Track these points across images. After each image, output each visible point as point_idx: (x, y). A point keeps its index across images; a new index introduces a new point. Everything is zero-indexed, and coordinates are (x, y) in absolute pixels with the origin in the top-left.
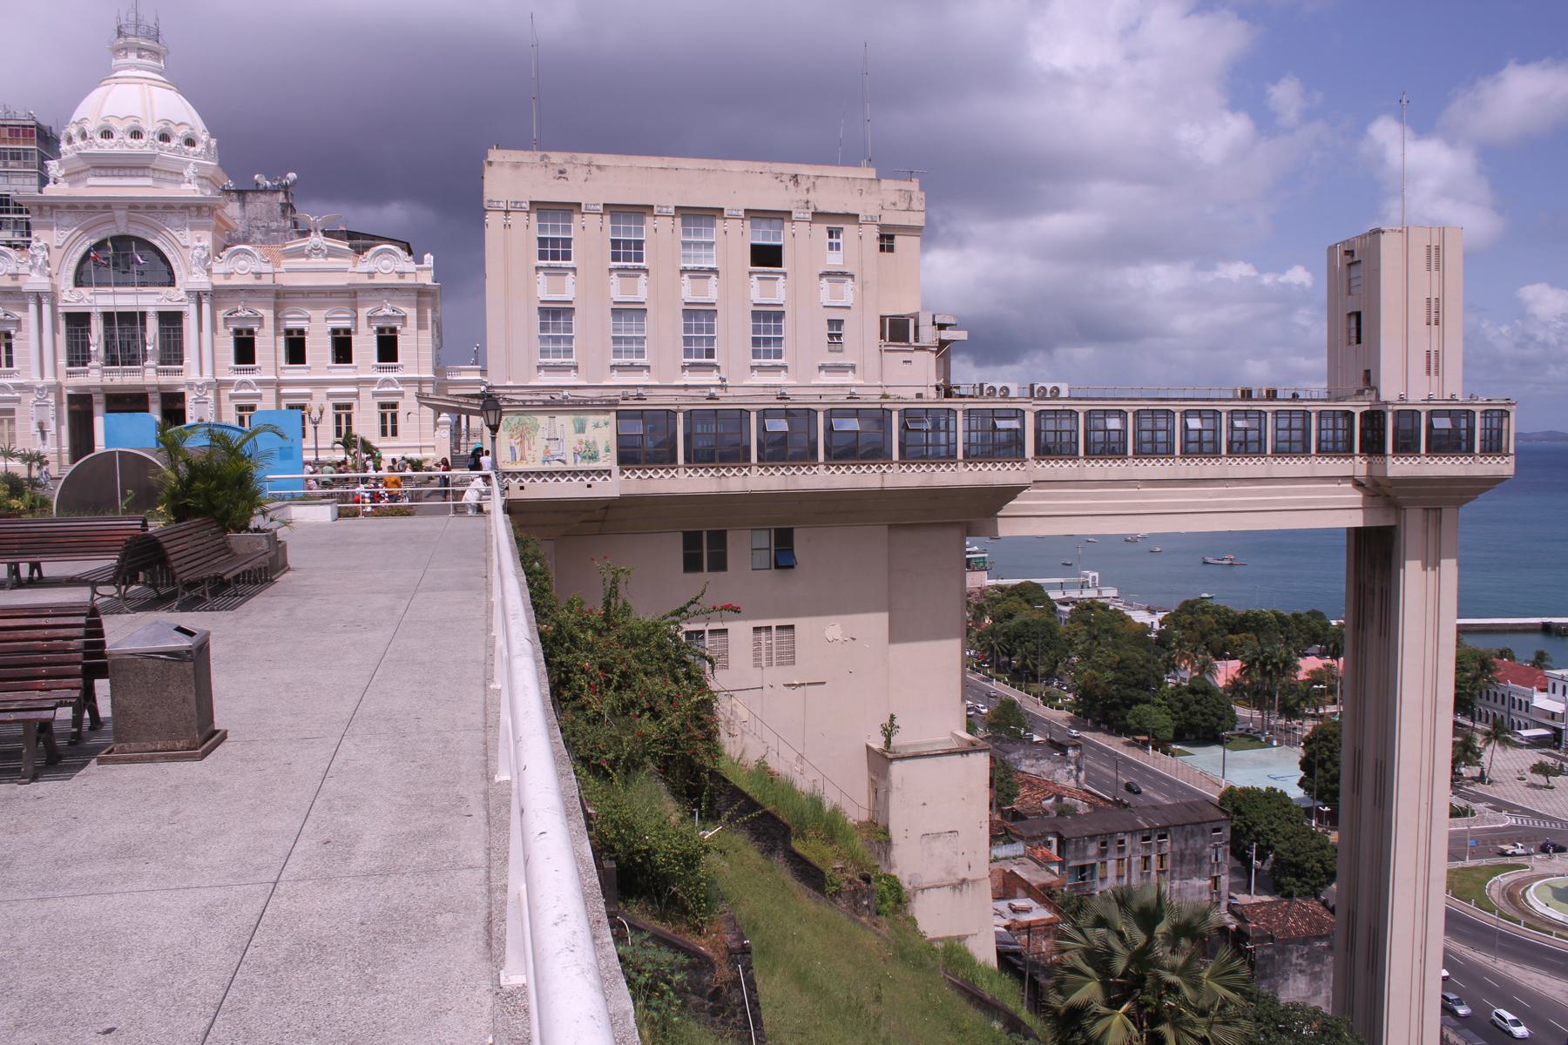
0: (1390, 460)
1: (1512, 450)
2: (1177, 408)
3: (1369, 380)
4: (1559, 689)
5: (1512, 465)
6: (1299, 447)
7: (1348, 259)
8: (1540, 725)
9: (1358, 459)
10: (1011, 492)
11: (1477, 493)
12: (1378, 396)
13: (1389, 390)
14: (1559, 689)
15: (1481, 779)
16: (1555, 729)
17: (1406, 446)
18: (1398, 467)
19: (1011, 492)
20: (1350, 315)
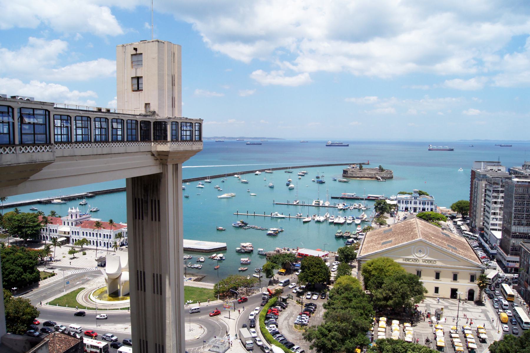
4: (66, 224)
7: (134, 52)
8: (62, 237)
9: (153, 143)
14: (66, 224)
16: (66, 237)
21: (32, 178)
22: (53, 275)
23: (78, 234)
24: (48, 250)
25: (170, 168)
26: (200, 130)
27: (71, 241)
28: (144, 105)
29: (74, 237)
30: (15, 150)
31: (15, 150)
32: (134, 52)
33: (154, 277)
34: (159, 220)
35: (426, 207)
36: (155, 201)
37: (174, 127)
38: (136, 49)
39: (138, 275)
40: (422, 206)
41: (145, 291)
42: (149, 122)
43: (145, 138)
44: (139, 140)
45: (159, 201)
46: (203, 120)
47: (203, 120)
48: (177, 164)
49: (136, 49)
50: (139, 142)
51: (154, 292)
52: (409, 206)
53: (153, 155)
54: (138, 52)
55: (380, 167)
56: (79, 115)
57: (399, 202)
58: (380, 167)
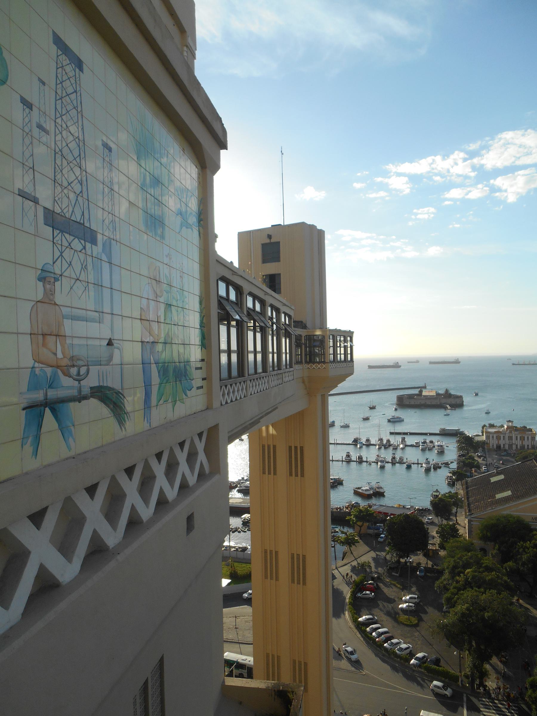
26: (351, 347)
32: (268, 241)
33: (293, 558)
34: (302, 475)
35: (526, 443)
36: (296, 448)
38: (270, 237)
39: (266, 557)
40: (519, 443)
41: (277, 579)
42: (301, 336)
46: (353, 333)
47: (353, 333)
49: (270, 237)
51: (293, 582)
52: (502, 442)
53: (303, 382)
54: (272, 241)
55: (447, 391)
57: (487, 437)
58: (447, 391)
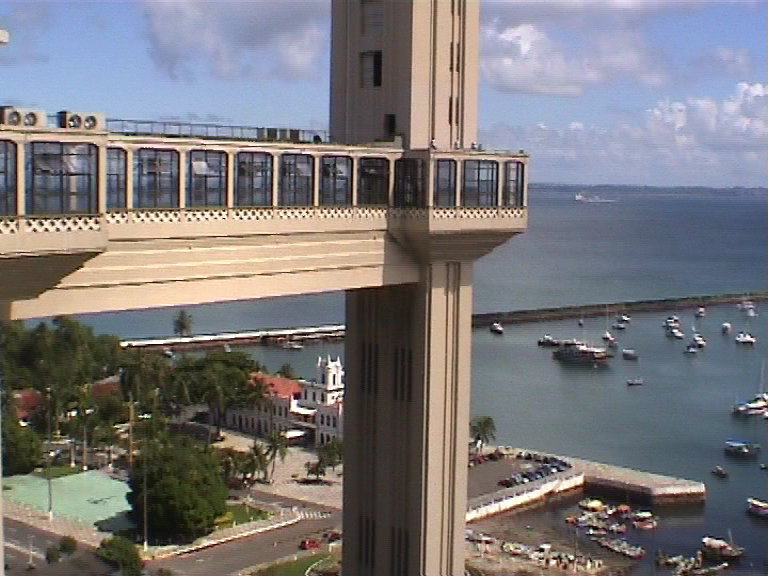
0: (432, 213)
1: (525, 204)
2: (183, 147)
3: (393, 127)
5: (525, 218)
6: (341, 197)
10: (75, 260)
11: (490, 247)
12: (406, 144)
13: (418, 140)
14: (310, 396)
15: (264, 481)
16: (307, 428)
17: (446, 198)
18: (441, 221)
19: (75, 260)
20: (362, 55)
21: (66, 282)
22: (259, 514)
23: (334, 425)
24: (254, 461)
25: (439, 270)
27: (318, 439)
28: (382, 120)
29: (324, 430)
30: (17, 225)
31: (17, 225)
34: (410, 398)
37: (444, 173)
43: (369, 199)
44: (355, 203)
45: (410, 353)
48: (459, 264)
50: (352, 207)
56: (198, 148)
